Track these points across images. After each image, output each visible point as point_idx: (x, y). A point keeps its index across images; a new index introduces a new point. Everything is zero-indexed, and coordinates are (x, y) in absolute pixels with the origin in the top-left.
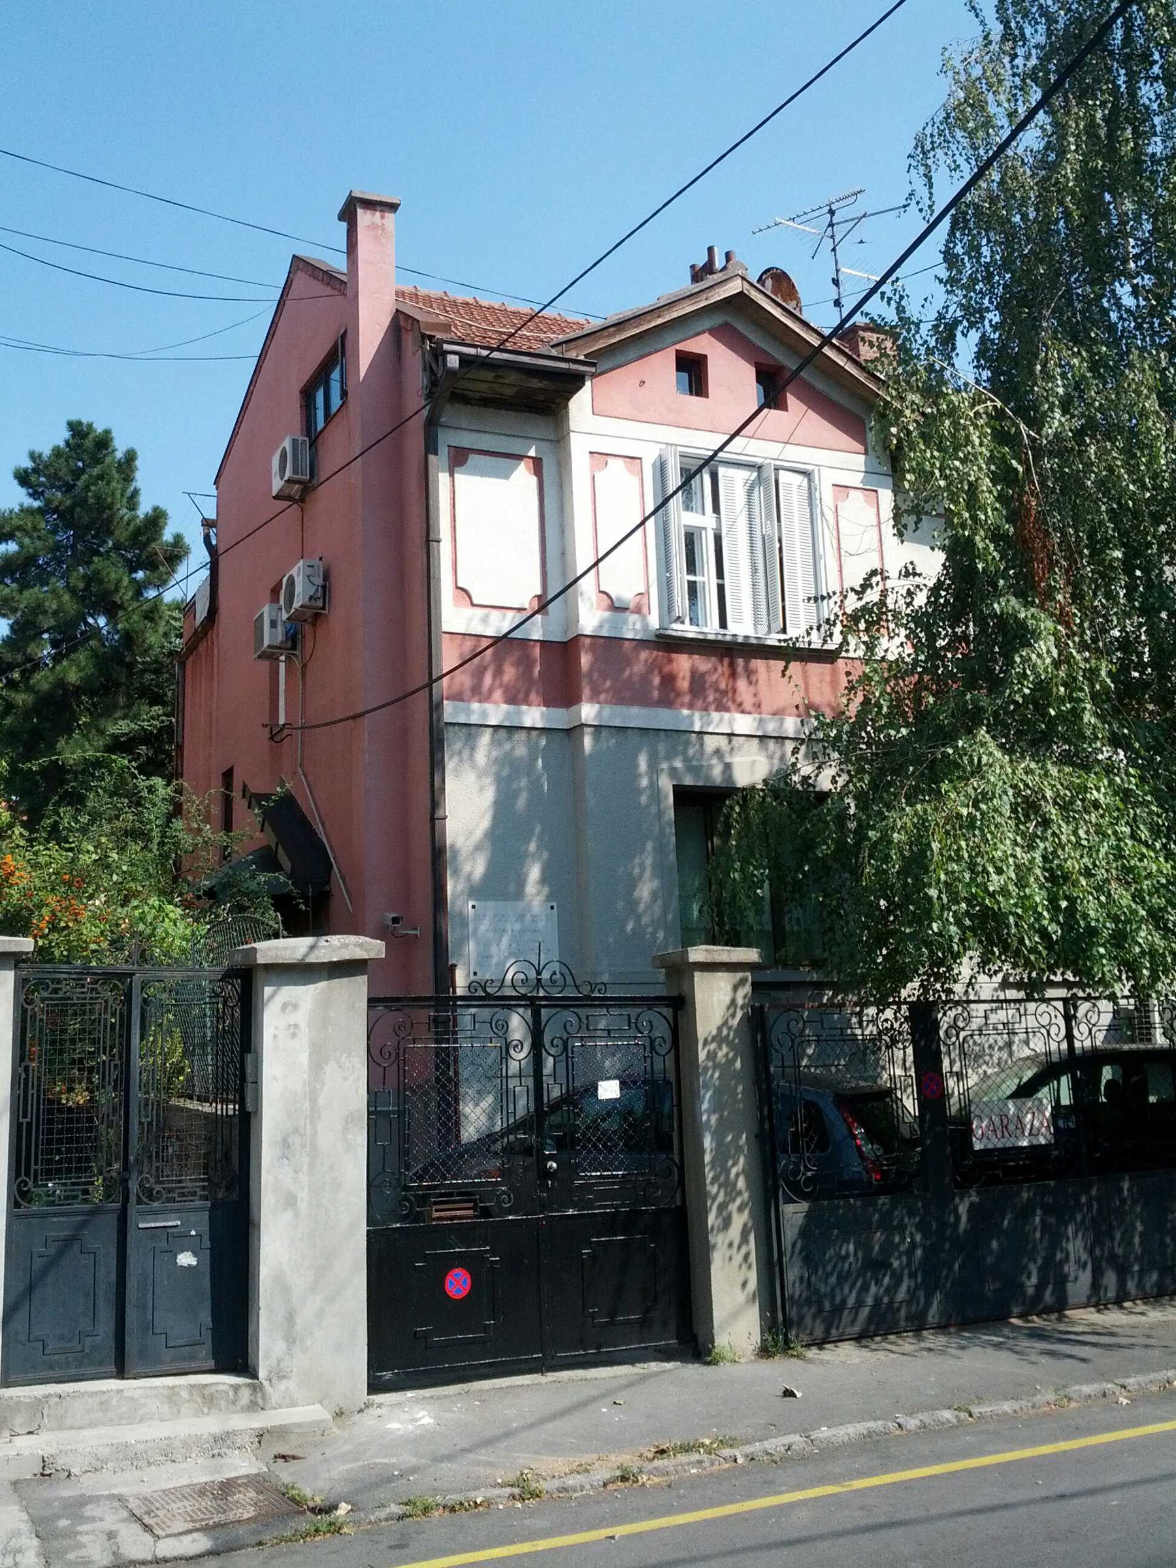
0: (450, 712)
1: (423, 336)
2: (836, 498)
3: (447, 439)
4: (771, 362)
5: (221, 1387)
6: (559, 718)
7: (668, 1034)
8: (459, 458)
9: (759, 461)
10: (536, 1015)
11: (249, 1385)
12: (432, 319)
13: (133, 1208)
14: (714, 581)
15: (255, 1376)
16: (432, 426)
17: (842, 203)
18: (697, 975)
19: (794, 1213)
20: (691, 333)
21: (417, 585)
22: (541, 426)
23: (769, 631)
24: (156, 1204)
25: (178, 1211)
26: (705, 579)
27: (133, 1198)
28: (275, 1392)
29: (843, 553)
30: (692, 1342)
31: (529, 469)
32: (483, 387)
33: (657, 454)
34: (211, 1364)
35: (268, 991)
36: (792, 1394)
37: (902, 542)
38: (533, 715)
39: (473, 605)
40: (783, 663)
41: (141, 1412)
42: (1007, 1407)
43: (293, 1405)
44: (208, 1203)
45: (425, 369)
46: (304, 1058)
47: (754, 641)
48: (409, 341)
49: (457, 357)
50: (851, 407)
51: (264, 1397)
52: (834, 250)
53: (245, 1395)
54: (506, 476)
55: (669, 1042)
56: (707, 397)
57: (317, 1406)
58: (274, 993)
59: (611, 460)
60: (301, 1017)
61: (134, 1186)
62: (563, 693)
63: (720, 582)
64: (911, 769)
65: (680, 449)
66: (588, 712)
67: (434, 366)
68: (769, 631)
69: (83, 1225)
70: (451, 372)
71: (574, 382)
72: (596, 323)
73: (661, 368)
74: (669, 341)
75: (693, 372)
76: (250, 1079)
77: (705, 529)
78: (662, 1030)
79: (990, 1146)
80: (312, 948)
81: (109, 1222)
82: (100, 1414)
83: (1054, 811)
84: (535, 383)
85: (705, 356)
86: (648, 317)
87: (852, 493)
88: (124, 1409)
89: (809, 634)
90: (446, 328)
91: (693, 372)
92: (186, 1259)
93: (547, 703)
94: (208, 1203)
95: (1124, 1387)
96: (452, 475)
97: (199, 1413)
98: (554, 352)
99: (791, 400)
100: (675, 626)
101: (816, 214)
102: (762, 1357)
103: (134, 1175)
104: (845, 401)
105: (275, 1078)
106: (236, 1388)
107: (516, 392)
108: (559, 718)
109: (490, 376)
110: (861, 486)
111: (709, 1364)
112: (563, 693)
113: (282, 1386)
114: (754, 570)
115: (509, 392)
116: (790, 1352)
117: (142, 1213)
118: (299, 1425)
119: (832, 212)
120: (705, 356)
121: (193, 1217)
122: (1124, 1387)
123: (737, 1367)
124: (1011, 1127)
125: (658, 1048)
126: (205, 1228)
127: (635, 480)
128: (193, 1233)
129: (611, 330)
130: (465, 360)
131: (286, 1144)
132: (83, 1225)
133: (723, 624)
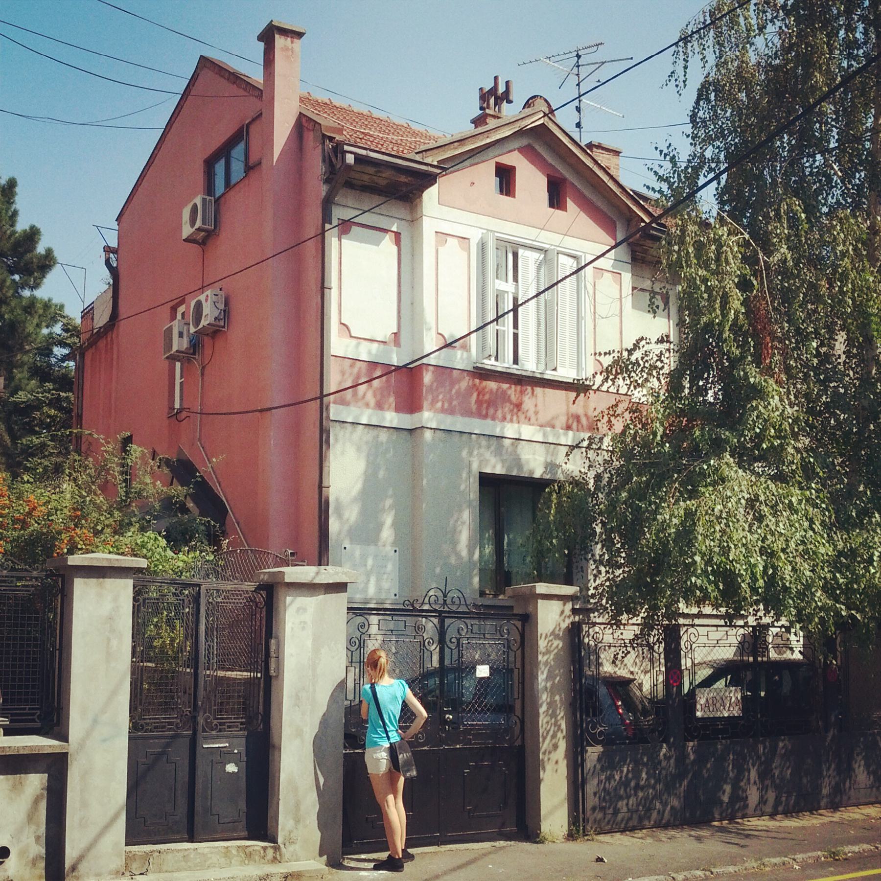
0: (335, 411)
1: (324, 136)
2: (594, 277)
3: (339, 213)
4: (557, 175)
5: (256, 848)
6: (404, 420)
7: (518, 639)
8: (345, 226)
9: (547, 246)
10: (442, 623)
11: (272, 847)
12: (331, 124)
13: (201, 734)
14: (511, 330)
15: (274, 840)
16: (327, 204)
17: (586, 51)
18: (539, 601)
19: (593, 752)
20: (505, 151)
21: (312, 316)
22: (399, 210)
23: (546, 369)
24: (214, 733)
25: (227, 737)
26: (505, 329)
27: (200, 729)
28: (286, 852)
29: (597, 316)
30: (526, 829)
31: (391, 240)
32: (366, 178)
33: (480, 236)
34: (245, 834)
35: (289, 599)
36: (601, 860)
37: (654, 317)
38: (391, 418)
39: (351, 336)
40: (575, 394)
41: (208, 863)
42: (731, 869)
43: (297, 860)
44: (246, 733)
45: (324, 161)
46: (309, 643)
47: (539, 376)
48: (310, 139)
49: (353, 156)
50: (605, 210)
51: (280, 855)
52: (578, 85)
53: (270, 853)
54: (377, 243)
55: (519, 643)
56: (514, 197)
57: (312, 861)
58: (292, 602)
59: (449, 239)
60: (308, 617)
61: (201, 720)
62: (410, 402)
63: (516, 331)
64: (676, 476)
65: (496, 234)
66: (428, 417)
67: (333, 160)
68: (546, 369)
69: (168, 745)
70: (349, 167)
71: (427, 179)
72: (449, 139)
73: (484, 173)
74: (491, 155)
75: (506, 178)
76: (273, 654)
77: (507, 292)
78: (515, 636)
79: (706, 716)
80: (317, 573)
81: (183, 745)
82: (183, 863)
83: (766, 510)
84: (403, 179)
85: (514, 168)
86: (481, 137)
87: (606, 274)
88: (198, 860)
89: (594, 377)
90: (340, 131)
91: (506, 178)
92: (231, 768)
93: (398, 410)
94: (246, 733)
95: (794, 860)
96: (340, 240)
97: (242, 863)
98: (418, 158)
99: (570, 203)
100: (486, 361)
101: (567, 56)
102: (568, 840)
103: (201, 714)
104: (599, 204)
105: (292, 655)
106: (265, 848)
107: (394, 184)
108: (404, 420)
109: (371, 170)
110: (611, 269)
111: (537, 843)
112: (410, 402)
113: (291, 848)
114: (539, 325)
115: (383, 182)
116: (586, 838)
117: (205, 738)
118: (308, 871)
119: (578, 56)
120: (514, 168)
121: (236, 741)
122: (794, 860)
123: (554, 845)
124: (718, 705)
125: (512, 647)
126: (243, 749)
127: (465, 254)
128: (236, 751)
129: (456, 144)
130: (359, 159)
131: (297, 697)
132: (168, 745)
133: (516, 361)
